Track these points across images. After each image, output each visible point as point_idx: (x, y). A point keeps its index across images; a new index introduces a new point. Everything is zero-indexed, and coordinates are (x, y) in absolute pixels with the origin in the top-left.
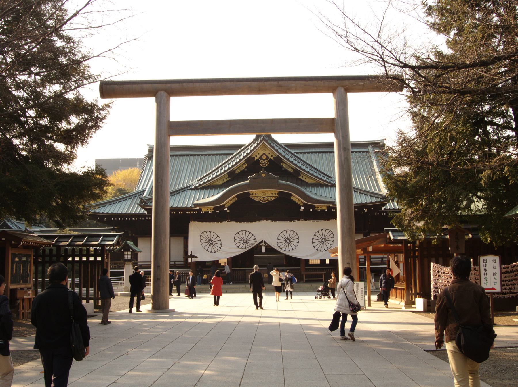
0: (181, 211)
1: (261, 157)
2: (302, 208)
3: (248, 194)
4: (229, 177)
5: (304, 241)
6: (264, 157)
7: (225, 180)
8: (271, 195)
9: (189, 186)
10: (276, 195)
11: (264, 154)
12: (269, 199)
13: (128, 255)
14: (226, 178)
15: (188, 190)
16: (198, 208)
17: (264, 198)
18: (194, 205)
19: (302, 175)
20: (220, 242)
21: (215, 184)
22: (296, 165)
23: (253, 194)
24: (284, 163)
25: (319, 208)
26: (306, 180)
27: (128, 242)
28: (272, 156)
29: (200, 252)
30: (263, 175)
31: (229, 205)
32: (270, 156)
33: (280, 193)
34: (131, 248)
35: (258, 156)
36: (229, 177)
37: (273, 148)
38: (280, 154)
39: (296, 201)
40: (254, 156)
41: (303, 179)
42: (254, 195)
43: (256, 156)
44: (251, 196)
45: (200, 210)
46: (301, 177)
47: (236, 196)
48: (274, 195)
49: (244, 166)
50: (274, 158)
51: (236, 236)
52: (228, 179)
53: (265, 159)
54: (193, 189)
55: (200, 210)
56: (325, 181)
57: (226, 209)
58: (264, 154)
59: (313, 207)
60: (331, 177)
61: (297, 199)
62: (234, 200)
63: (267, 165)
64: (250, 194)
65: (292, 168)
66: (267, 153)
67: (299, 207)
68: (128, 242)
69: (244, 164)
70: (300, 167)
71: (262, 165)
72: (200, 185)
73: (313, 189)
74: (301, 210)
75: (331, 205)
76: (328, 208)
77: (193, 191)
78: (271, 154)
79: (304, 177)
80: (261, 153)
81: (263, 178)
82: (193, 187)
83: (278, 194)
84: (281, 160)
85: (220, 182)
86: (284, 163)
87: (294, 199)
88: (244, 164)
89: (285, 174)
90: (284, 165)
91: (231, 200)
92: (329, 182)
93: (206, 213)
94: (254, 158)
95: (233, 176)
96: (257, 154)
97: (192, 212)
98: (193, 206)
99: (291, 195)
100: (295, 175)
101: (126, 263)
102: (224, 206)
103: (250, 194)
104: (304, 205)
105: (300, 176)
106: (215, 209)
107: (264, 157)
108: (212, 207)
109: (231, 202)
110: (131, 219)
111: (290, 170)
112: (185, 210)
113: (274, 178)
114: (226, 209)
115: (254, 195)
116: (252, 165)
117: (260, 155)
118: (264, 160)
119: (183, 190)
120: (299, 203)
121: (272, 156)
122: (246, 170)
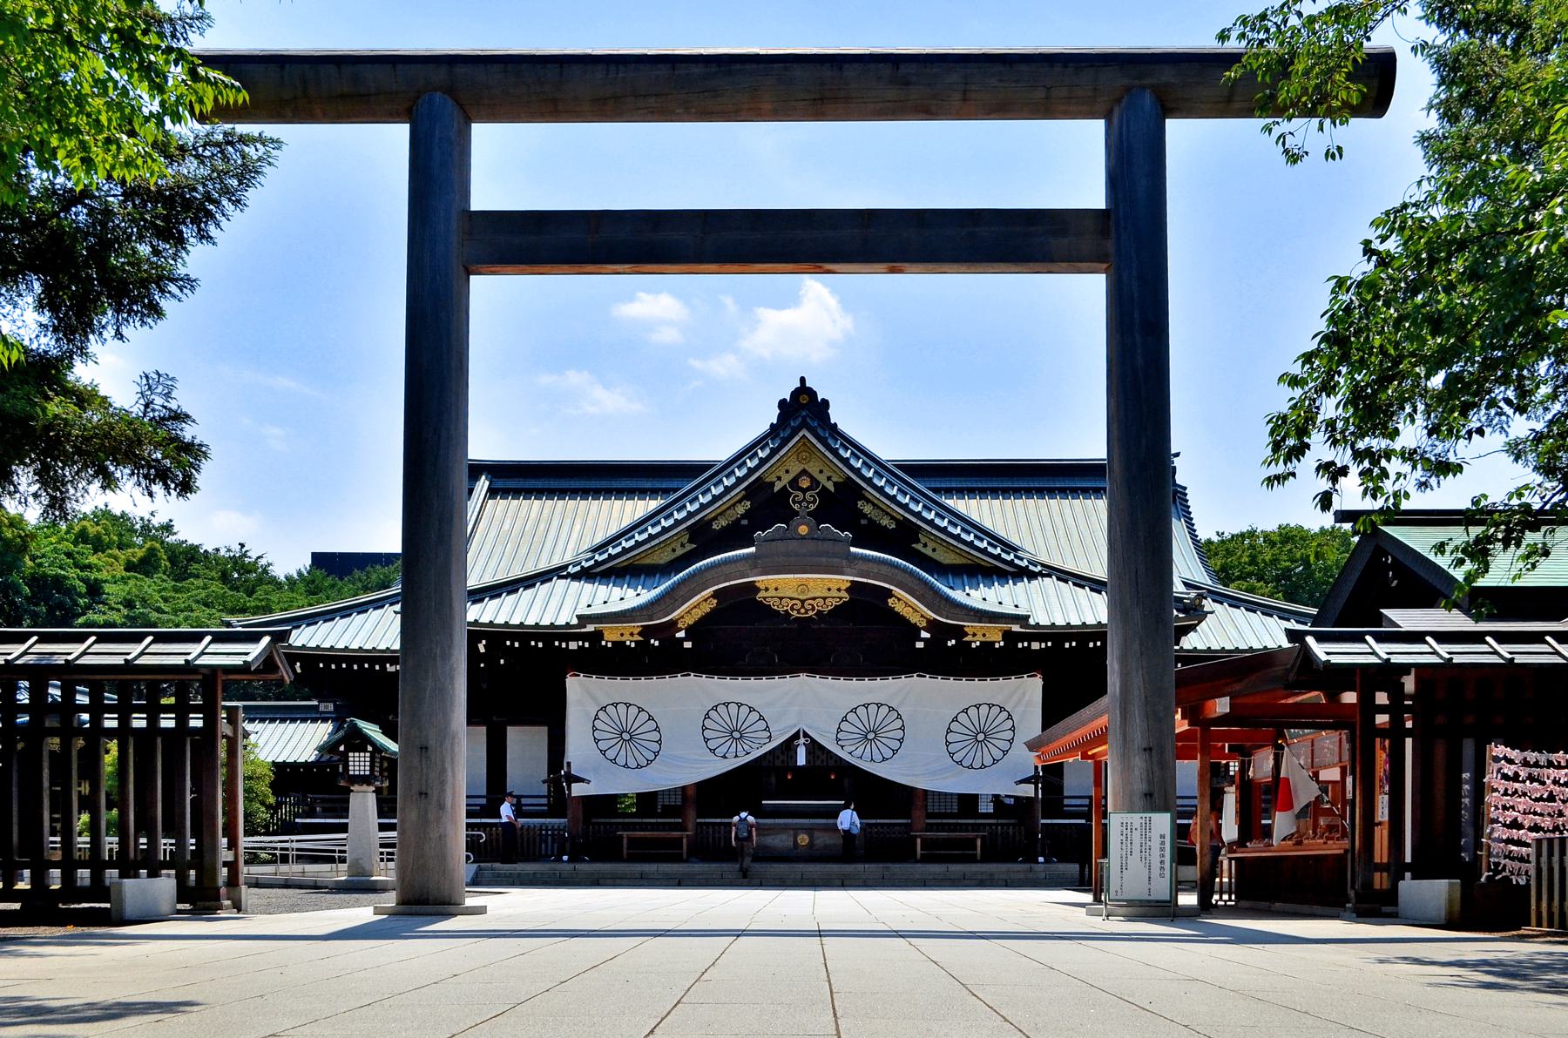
0: (537, 637)
1: (794, 482)
2: (924, 635)
3: (752, 588)
4: (690, 541)
5: (933, 734)
6: (805, 483)
7: (680, 552)
9: (566, 567)
11: (804, 472)
12: (819, 605)
13: (359, 763)
14: (683, 545)
15: (560, 577)
16: (590, 628)
17: (803, 602)
18: (579, 617)
19: (923, 539)
20: (659, 734)
21: (647, 561)
22: (905, 507)
24: (868, 501)
25: (979, 634)
26: (935, 556)
27: (361, 724)
28: (829, 478)
29: (598, 772)
30: (803, 530)
31: (690, 620)
32: (822, 479)
33: (854, 588)
34: (367, 740)
35: (786, 479)
36: (690, 541)
37: (835, 452)
38: (857, 472)
40: (772, 478)
41: (928, 551)
43: (779, 478)
44: (762, 594)
45: (598, 635)
46: (919, 547)
47: (716, 595)
48: (834, 593)
49: (741, 510)
50: (835, 484)
51: (707, 716)
52: (689, 547)
53: (808, 489)
54: (576, 577)
55: (598, 635)
56: (997, 558)
57: (681, 634)
58: (804, 472)
59: (959, 632)
60: (1015, 550)
61: (907, 605)
62: (706, 608)
63: (812, 507)
64: (758, 590)
65: (893, 518)
66: (813, 469)
68: (361, 724)
69: (740, 501)
70: (918, 515)
71: (796, 507)
72: (598, 564)
73: (958, 581)
74: (920, 645)
75: (1016, 628)
76: (1007, 635)
77: (575, 584)
78: (827, 473)
79: (931, 545)
80: (795, 469)
81: (803, 538)
82: (578, 568)
83: (847, 590)
84: (858, 493)
85: (664, 557)
86: (868, 501)
87: (899, 608)
88: (740, 501)
89: (870, 535)
90: (867, 509)
91: (697, 606)
92: (1011, 563)
93: (619, 645)
94: (773, 484)
95: (705, 538)
96: (781, 474)
97: (573, 645)
98: (575, 621)
99: (889, 593)
100: (902, 538)
101: (355, 788)
102: (673, 625)
103: (758, 590)
104: (932, 625)
105: (918, 541)
106: (647, 632)
107: (805, 483)
108: (636, 626)
109: (698, 614)
110: (383, 668)
111: (885, 522)
112: (550, 634)
113: (837, 540)
114: (681, 634)
115: (772, 593)
116: (766, 505)
117: (791, 476)
118: (804, 491)
119: (545, 576)
121: (829, 478)
122: (745, 522)
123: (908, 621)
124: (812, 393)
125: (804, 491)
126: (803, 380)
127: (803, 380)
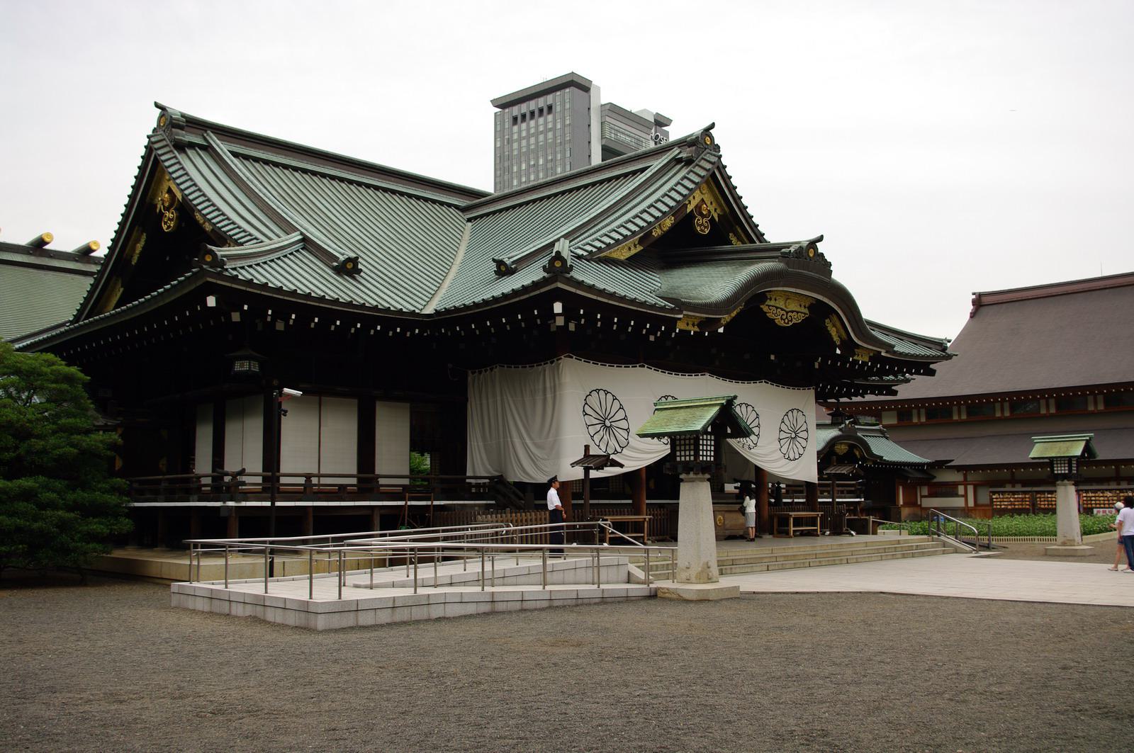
1: (698, 207)
7: (633, 251)
8: (798, 309)
10: (806, 311)
14: (635, 246)
17: (787, 313)
23: (771, 299)
39: (833, 332)
42: (772, 303)
44: (768, 302)
52: (640, 248)
67: (834, 346)
71: (698, 229)
85: (623, 254)
114: (721, 330)
115: (772, 303)
120: (836, 338)
121: (715, 210)
123: (832, 339)
124: (712, 139)
125: (703, 216)
126: (713, 126)
127: (713, 126)
